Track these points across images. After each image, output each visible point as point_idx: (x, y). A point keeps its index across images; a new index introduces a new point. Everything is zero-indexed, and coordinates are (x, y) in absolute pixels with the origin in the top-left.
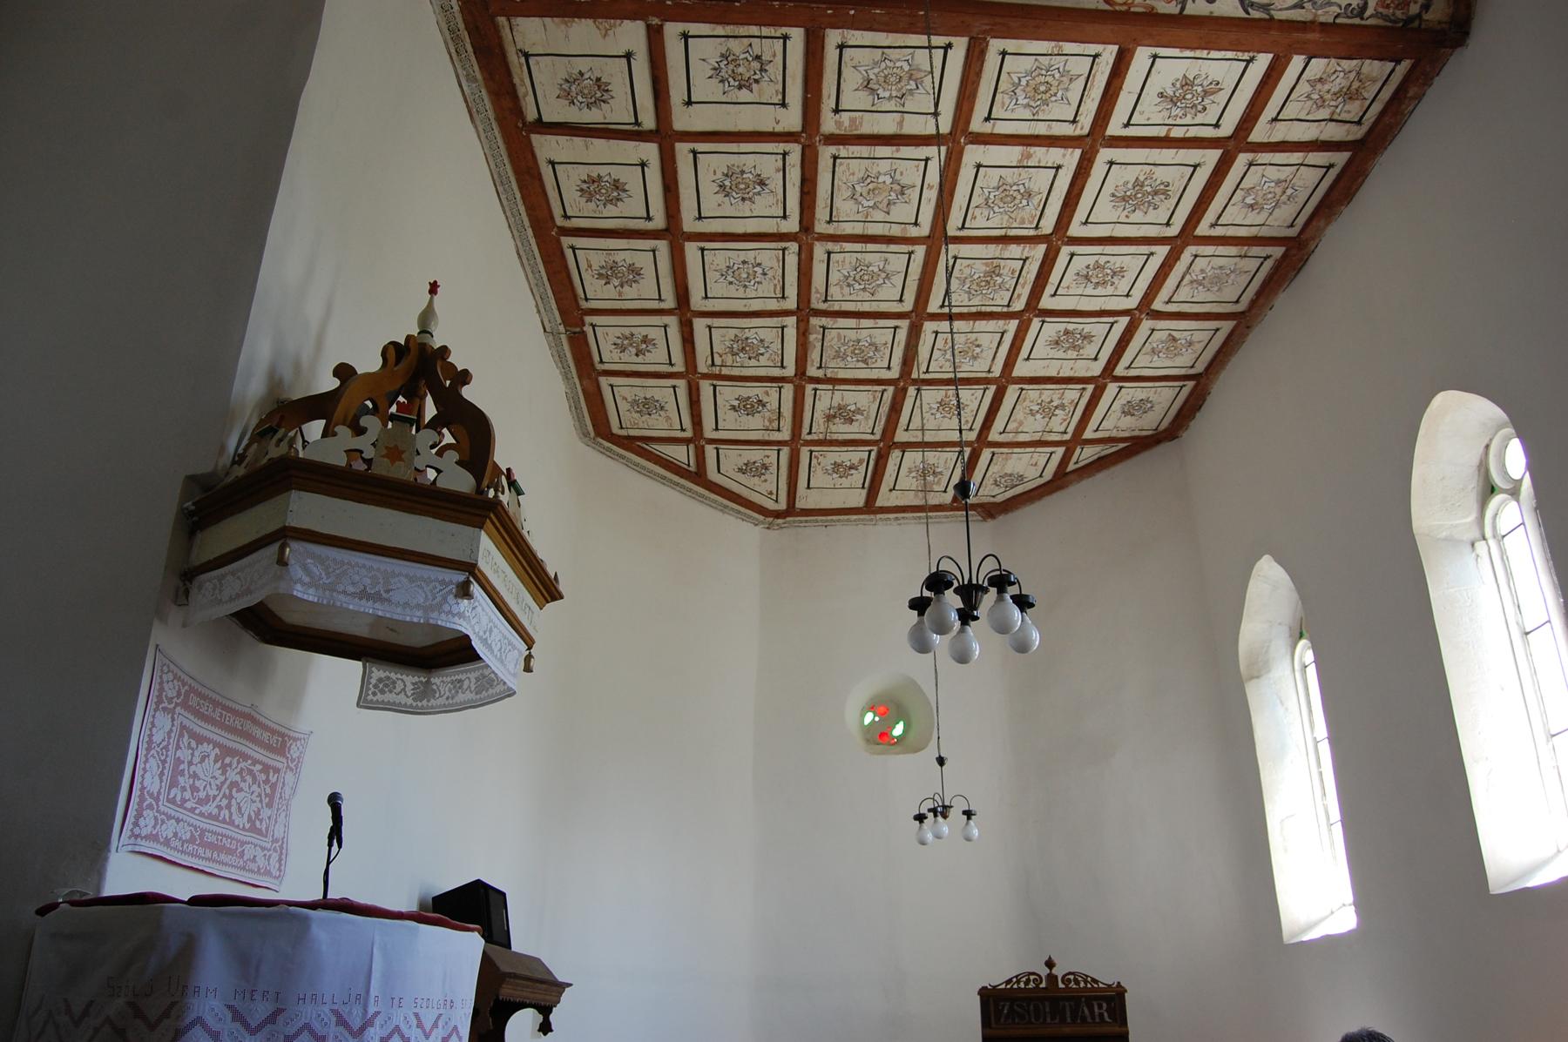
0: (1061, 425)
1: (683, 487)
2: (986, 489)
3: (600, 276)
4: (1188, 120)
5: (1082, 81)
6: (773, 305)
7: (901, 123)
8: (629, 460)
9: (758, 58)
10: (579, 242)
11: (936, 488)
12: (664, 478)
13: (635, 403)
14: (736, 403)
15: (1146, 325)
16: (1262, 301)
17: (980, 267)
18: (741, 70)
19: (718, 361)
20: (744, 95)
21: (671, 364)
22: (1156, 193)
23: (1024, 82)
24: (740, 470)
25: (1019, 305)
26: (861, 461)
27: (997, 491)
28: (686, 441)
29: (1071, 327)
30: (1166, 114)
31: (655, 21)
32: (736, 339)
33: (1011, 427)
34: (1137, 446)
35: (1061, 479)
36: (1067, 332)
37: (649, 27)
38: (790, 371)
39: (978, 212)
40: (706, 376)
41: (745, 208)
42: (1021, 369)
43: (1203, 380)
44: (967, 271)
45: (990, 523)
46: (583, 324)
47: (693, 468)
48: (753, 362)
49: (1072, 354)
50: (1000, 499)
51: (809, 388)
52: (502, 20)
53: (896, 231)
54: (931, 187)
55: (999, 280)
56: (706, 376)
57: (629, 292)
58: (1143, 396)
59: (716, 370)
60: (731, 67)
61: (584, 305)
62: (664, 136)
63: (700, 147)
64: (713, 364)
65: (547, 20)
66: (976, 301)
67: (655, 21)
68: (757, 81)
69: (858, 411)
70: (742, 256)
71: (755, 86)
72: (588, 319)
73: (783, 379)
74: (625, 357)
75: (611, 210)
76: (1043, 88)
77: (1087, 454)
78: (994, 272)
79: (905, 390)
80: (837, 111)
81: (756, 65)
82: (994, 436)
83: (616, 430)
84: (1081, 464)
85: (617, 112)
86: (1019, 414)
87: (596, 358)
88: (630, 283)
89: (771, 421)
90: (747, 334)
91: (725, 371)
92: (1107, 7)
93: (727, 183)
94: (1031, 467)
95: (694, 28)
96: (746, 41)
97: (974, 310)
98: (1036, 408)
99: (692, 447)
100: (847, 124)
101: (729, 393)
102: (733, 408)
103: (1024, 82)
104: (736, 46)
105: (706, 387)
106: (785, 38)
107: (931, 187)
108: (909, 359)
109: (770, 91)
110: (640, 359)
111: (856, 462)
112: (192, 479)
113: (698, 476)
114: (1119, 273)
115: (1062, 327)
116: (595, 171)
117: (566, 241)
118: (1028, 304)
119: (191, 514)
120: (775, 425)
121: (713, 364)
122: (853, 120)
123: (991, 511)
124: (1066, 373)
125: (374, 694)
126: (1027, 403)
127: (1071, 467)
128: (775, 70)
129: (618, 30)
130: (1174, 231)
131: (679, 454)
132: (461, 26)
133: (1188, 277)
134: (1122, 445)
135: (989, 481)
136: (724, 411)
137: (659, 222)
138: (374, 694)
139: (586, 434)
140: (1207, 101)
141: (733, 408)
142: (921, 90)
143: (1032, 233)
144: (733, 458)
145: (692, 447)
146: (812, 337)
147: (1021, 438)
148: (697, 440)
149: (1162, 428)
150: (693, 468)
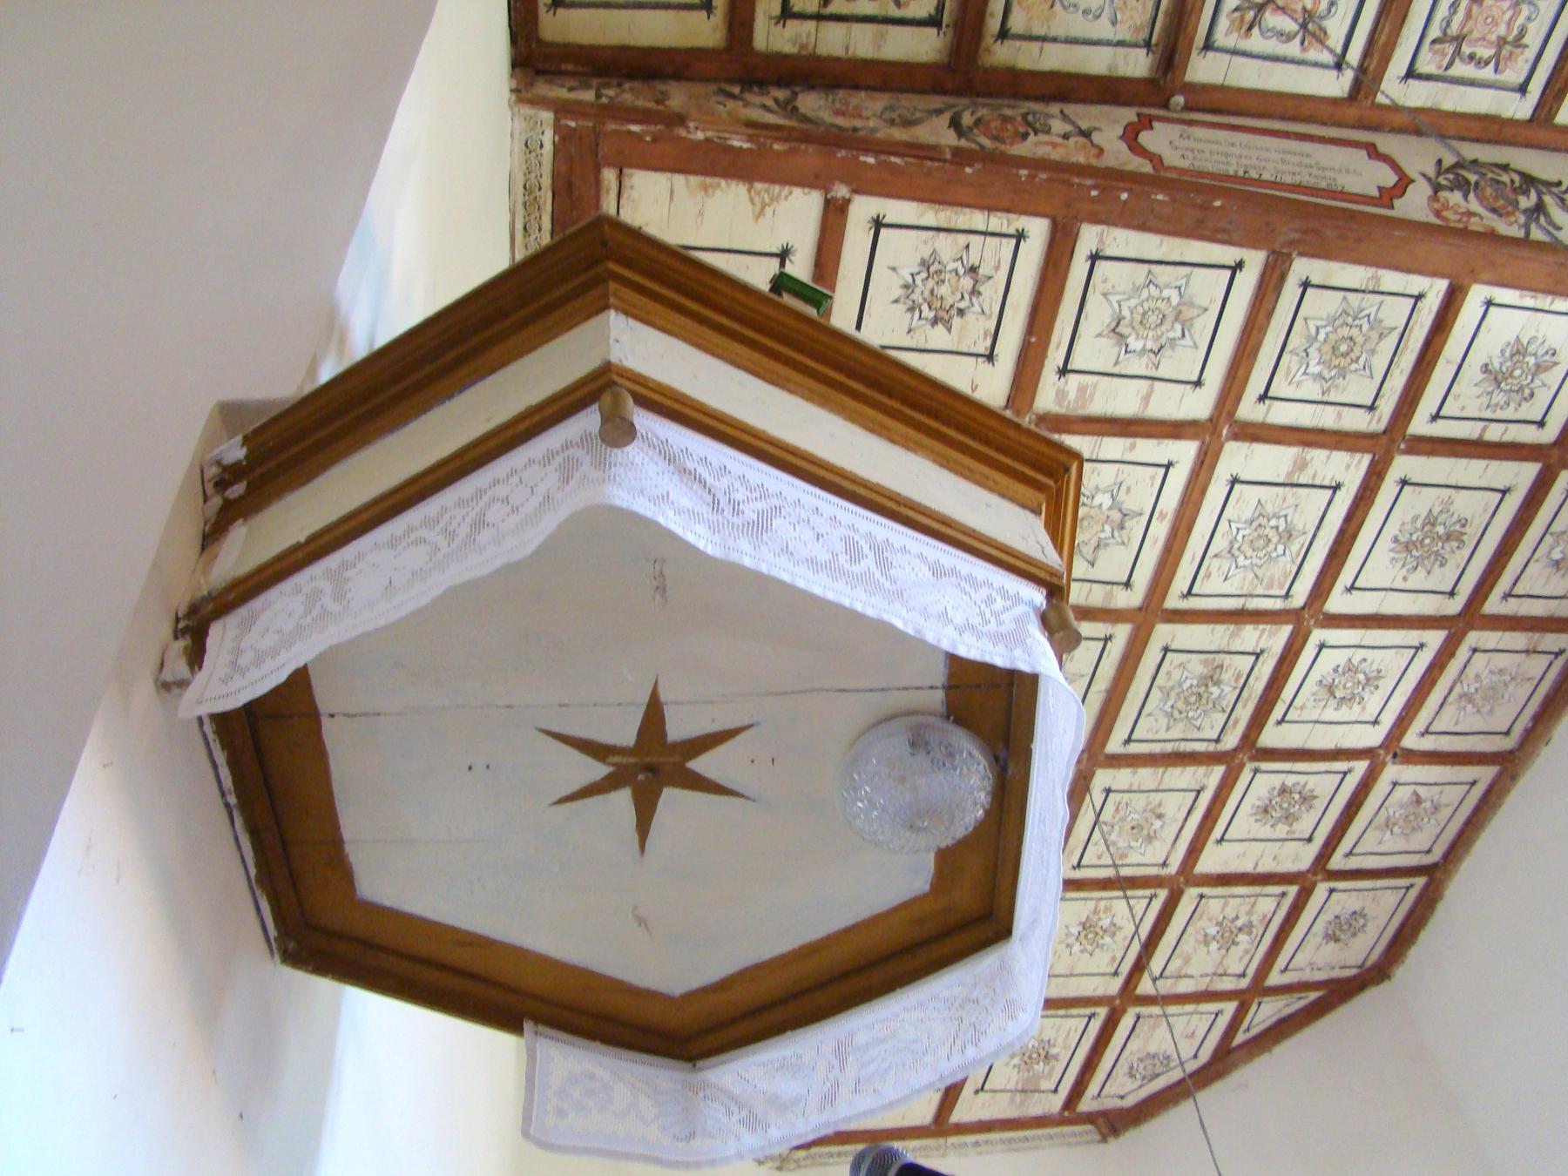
0: (1240, 962)
2: (1117, 1086)
4: (1509, 413)
5: (1395, 337)
7: (1146, 399)
9: (973, 270)
15: (1392, 771)
16: (1540, 727)
17: (1196, 666)
18: (944, 290)
22: (1449, 537)
23: (1321, 337)
29: (1291, 780)
30: (1485, 400)
31: (841, 191)
33: (1172, 967)
34: (1337, 992)
35: (1224, 1059)
36: (1284, 790)
37: (828, 203)
39: (1216, 563)
43: (1438, 875)
44: (1176, 675)
45: (1114, 1145)
49: (1282, 830)
50: (1130, 1101)
52: (609, 175)
54: (1163, 516)
55: (1215, 690)
58: (1357, 906)
60: (931, 283)
65: (679, 180)
66: (1175, 733)
67: (841, 191)
68: (961, 312)
71: (956, 321)
76: (1343, 348)
77: (1266, 1012)
78: (1211, 679)
80: (1064, 371)
81: (967, 283)
84: (1254, 1032)
86: (1188, 945)
92: (1439, 222)
94: (1185, 1036)
96: (962, 239)
97: (1169, 747)
98: (1212, 930)
100: (1072, 396)
103: (1321, 337)
104: (947, 246)
106: (1020, 236)
107: (1163, 516)
109: (974, 331)
112: (229, 413)
114: (1371, 681)
115: (1276, 780)
119: (229, 475)
122: (1082, 389)
123: (1113, 1123)
124: (1266, 866)
125: (561, 1112)
126: (1203, 923)
127: (1240, 1037)
128: (991, 293)
129: (782, 206)
130: (1454, 606)
132: (546, 181)
133: (1457, 689)
134: (1313, 996)
135: (1122, 1068)
138: (561, 1112)
140: (1537, 382)
142: (1188, 341)
143: (1277, 604)
147: (1185, 987)
149: (1369, 963)
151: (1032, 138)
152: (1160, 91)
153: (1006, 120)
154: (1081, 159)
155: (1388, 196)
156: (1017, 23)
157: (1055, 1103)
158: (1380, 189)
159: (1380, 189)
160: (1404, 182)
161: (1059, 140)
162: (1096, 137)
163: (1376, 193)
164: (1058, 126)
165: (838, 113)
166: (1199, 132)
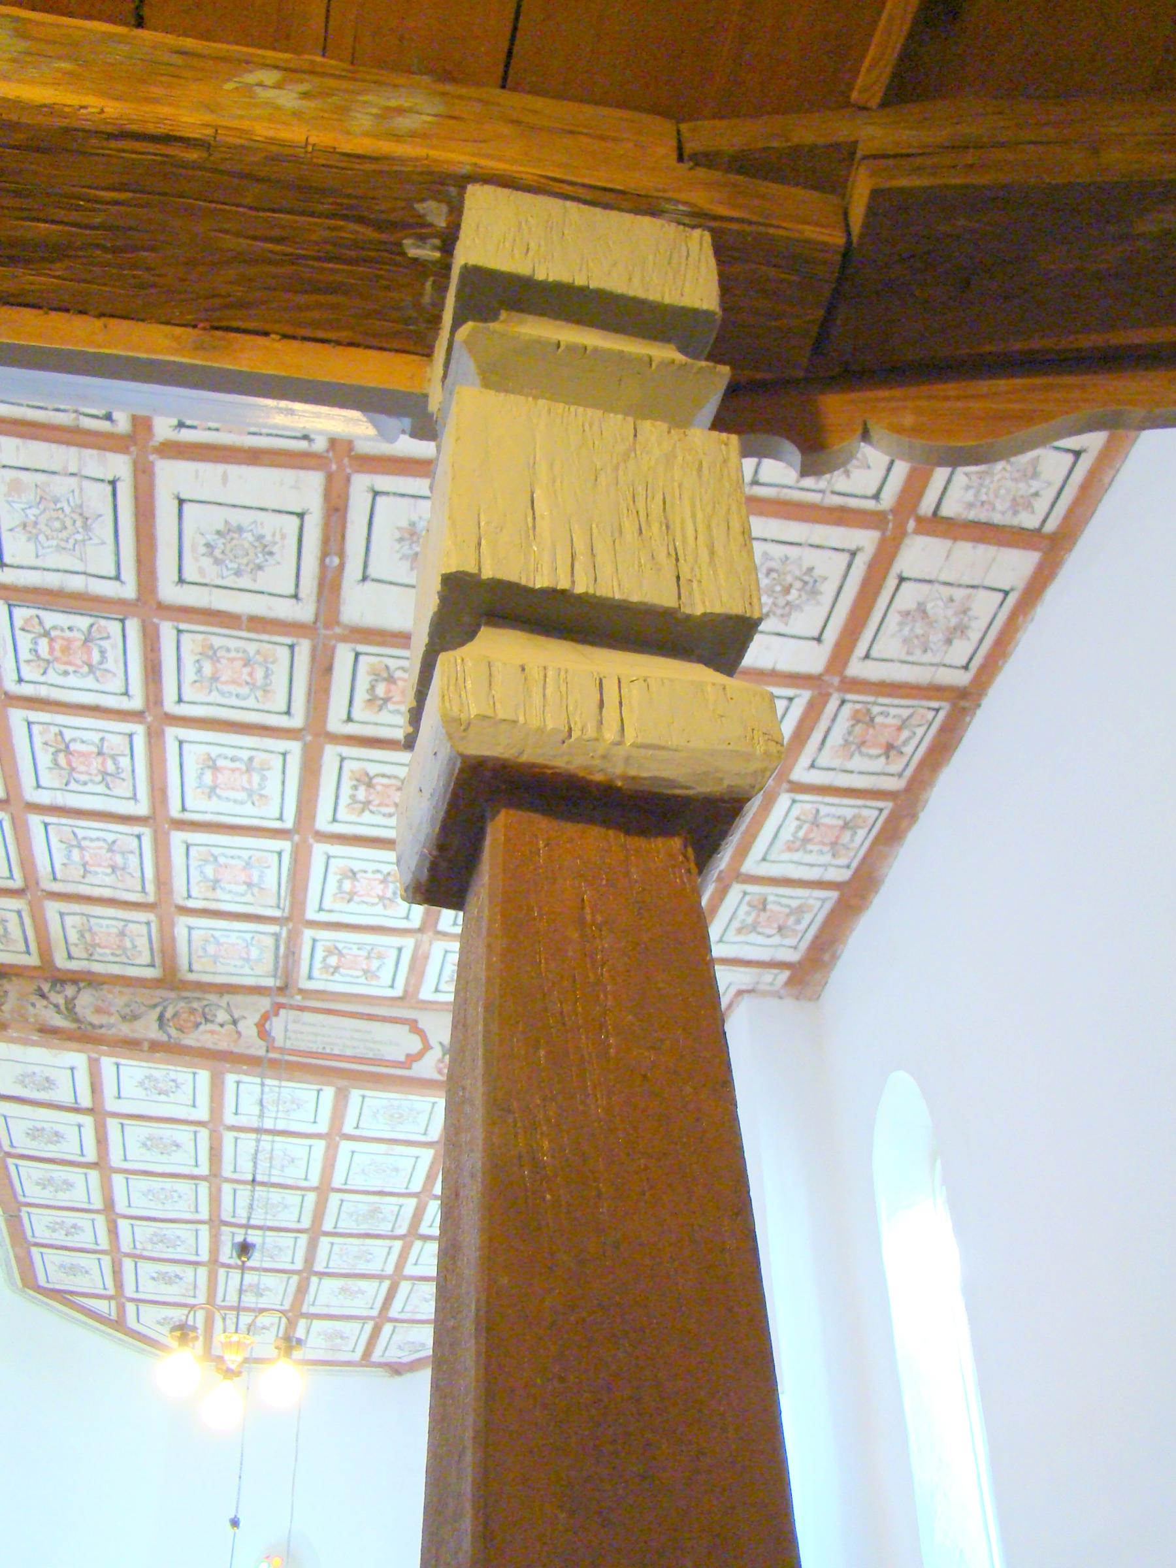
1: (103, 1332)
3: (38, 1184)
6: (188, 1216)
8: (52, 1307)
9: (173, 1081)
10: (20, 1162)
11: (344, 1348)
12: (85, 1323)
13: (62, 1266)
14: (155, 1275)
19: (138, 1245)
20: (163, 1098)
21: (97, 1244)
24: (159, 1323)
25: (402, 1230)
26: (272, 1324)
27: (401, 1354)
28: (109, 1298)
32: (155, 1234)
33: (408, 1308)
38: (205, 1256)
40: (128, 1255)
41: (164, 1158)
42: (409, 1270)
46: (20, 1211)
47: (114, 1316)
48: (170, 1250)
50: (406, 1360)
51: (222, 1272)
53: (290, 1182)
55: (380, 1215)
56: (128, 1255)
57: (61, 1195)
59: (138, 1252)
61: (21, 1199)
62: (97, 1111)
63: (126, 1122)
64: (135, 1247)
67: (95, 1055)
69: (268, 1289)
70: (161, 1185)
72: (24, 1209)
73: (196, 1264)
74: (55, 1235)
75: (51, 1147)
79: (308, 1279)
81: (173, 1084)
82: (394, 1312)
83: (42, 1281)
85: (63, 1095)
87: (29, 1233)
88: (64, 1191)
89: (186, 1289)
90: (165, 1232)
91: (145, 1253)
93: (149, 1143)
95: (122, 1061)
99: (113, 1303)
101: (146, 1268)
102: (153, 1278)
105: (128, 1264)
108: (310, 1258)
110: (70, 1238)
111: (267, 1324)
113: (118, 1324)
116: (39, 1125)
117: (10, 1161)
118: (409, 1231)
120: (191, 1293)
121: (135, 1247)
131: (102, 1306)
136: (143, 1280)
137: (91, 1155)
139: (14, 1284)
141: (153, 1278)
144: (150, 1315)
145: (113, 1303)
146: (223, 1238)
148: (119, 1295)
150: (114, 1316)
151: (202, 1028)
152: (284, 992)
153: (192, 1011)
154: (223, 1046)
155: (412, 1059)
156: (195, 967)
157: (357, 1356)
158: (408, 1056)
159: (408, 1056)
160: (427, 1047)
161: (218, 1028)
162: (241, 1026)
163: (402, 1058)
164: (222, 1016)
165: (99, 1011)
166: (308, 1017)
